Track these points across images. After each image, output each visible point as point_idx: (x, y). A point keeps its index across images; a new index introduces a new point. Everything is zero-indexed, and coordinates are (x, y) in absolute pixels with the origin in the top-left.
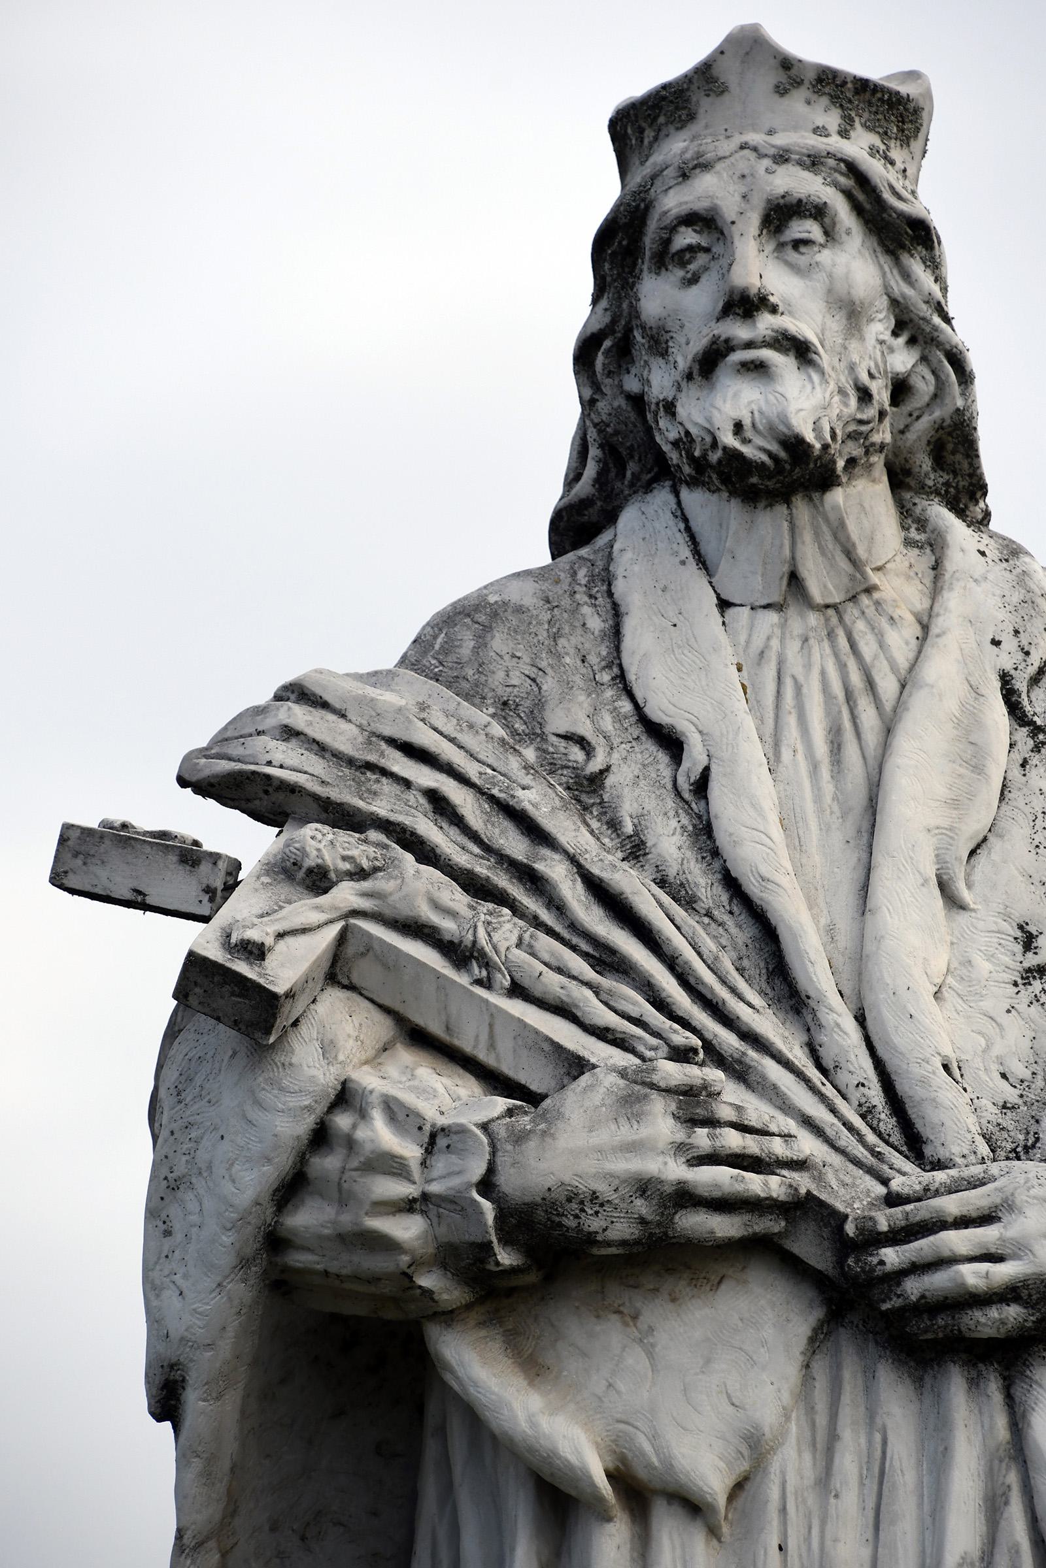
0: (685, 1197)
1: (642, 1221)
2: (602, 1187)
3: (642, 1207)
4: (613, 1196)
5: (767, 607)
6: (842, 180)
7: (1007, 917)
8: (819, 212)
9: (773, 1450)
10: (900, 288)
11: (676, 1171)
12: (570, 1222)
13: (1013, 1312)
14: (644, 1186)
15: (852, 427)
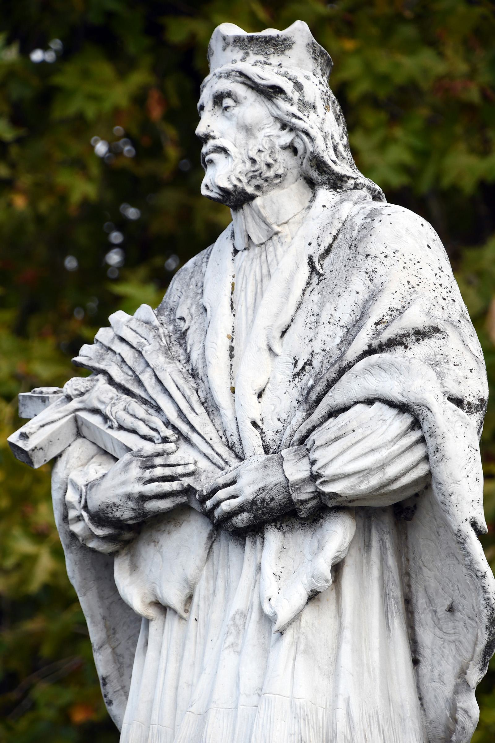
0: (143, 498)
1: (133, 509)
2: (116, 501)
3: (131, 504)
4: (120, 503)
5: (245, 249)
6: (239, 79)
7: (289, 355)
8: (229, 95)
9: (195, 583)
10: (276, 112)
11: (138, 488)
12: (110, 515)
13: (245, 516)
14: (129, 497)
15: (251, 174)
